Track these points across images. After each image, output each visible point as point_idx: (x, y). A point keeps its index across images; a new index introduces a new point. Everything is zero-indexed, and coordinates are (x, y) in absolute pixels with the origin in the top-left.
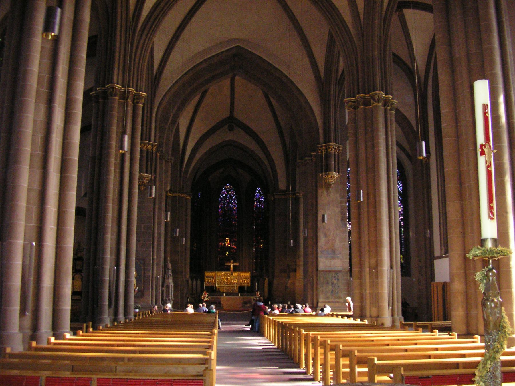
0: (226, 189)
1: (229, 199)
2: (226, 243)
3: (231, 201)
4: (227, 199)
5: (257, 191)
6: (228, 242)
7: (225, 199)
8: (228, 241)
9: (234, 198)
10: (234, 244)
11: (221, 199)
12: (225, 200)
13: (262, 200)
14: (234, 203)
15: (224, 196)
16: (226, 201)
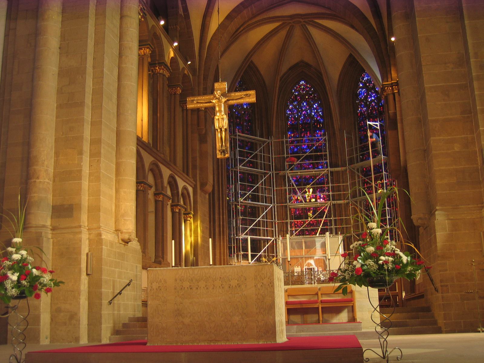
0: (299, 91)
1: (306, 111)
2: (306, 196)
3: (311, 112)
4: (302, 111)
5: (361, 85)
6: (311, 193)
7: (297, 109)
8: (309, 192)
9: (315, 106)
10: (322, 196)
11: (290, 110)
12: (298, 112)
13: (372, 101)
14: (318, 116)
15: (295, 106)
16: (301, 114)
